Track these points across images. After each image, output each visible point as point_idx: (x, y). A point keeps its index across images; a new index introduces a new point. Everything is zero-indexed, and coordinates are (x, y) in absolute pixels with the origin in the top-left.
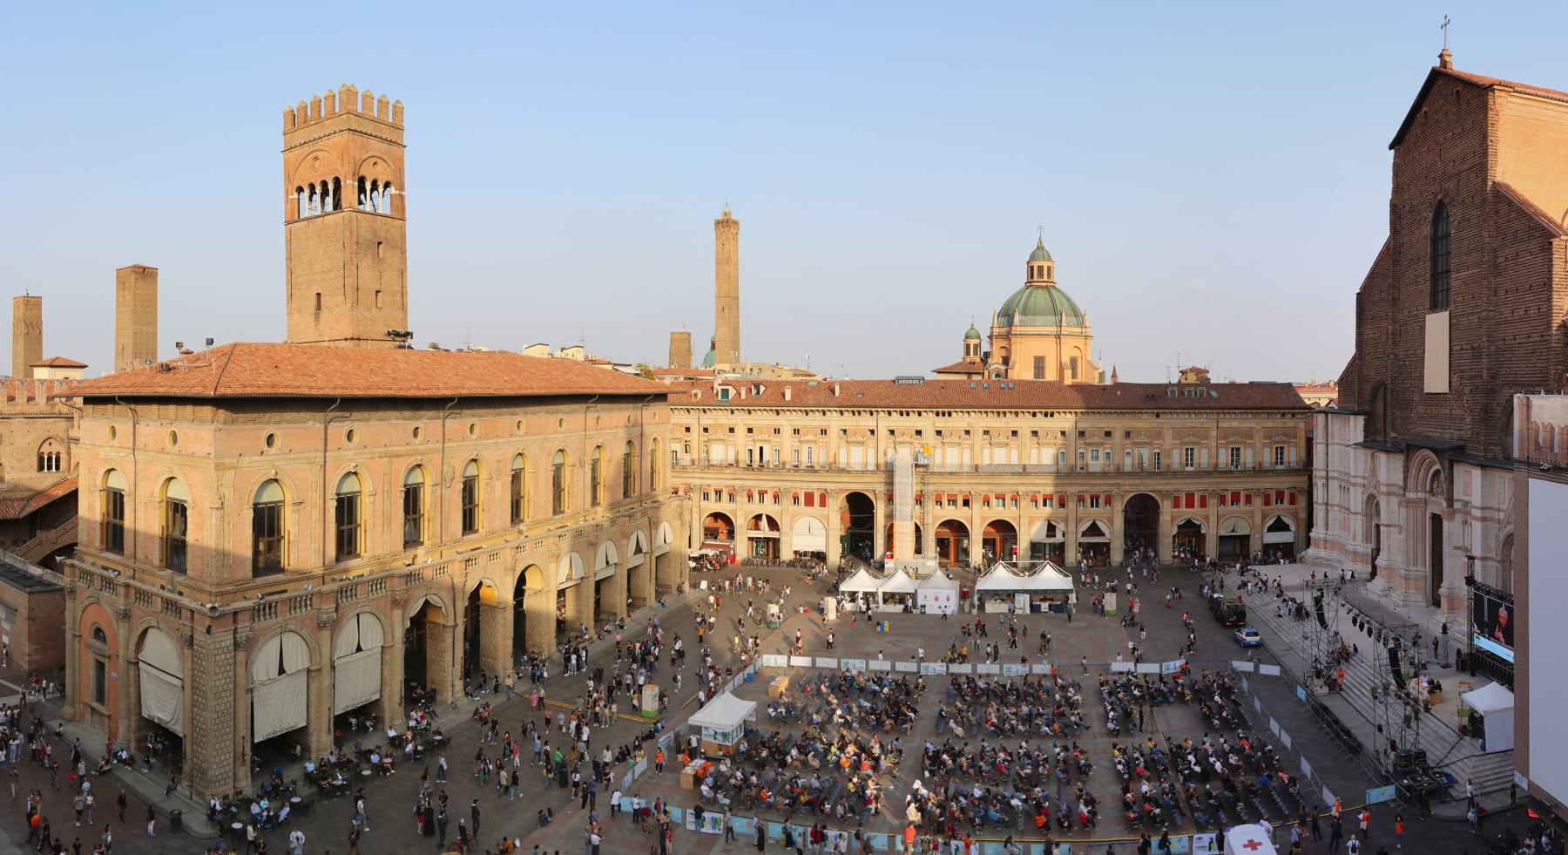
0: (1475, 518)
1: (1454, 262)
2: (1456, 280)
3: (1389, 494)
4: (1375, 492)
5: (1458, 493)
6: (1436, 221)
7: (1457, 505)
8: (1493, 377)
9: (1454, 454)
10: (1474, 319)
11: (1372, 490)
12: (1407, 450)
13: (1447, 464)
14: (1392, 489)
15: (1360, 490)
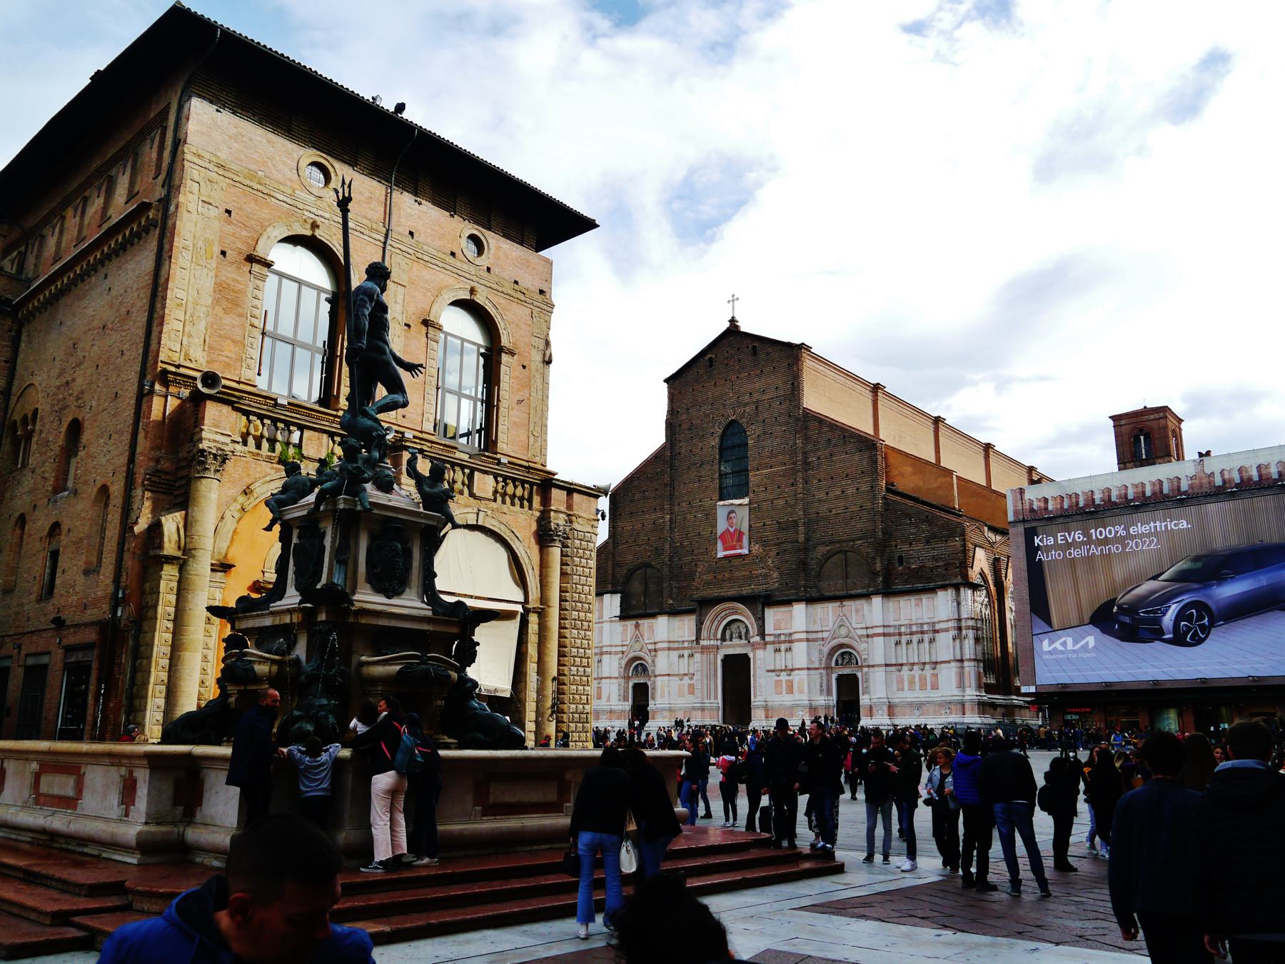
0: (800, 640)
1: (752, 464)
2: (754, 478)
3: (669, 649)
4: (641, 654)
5: (769, 629)
6: (723, 437)
7: (767, 638)
8: (807, 540)
9: (760, 602)
10: (782, 502)
11: (631, 655)
12: (700, 607)
13: (760, 607)
14: (672, 645)
15: (615, 658)
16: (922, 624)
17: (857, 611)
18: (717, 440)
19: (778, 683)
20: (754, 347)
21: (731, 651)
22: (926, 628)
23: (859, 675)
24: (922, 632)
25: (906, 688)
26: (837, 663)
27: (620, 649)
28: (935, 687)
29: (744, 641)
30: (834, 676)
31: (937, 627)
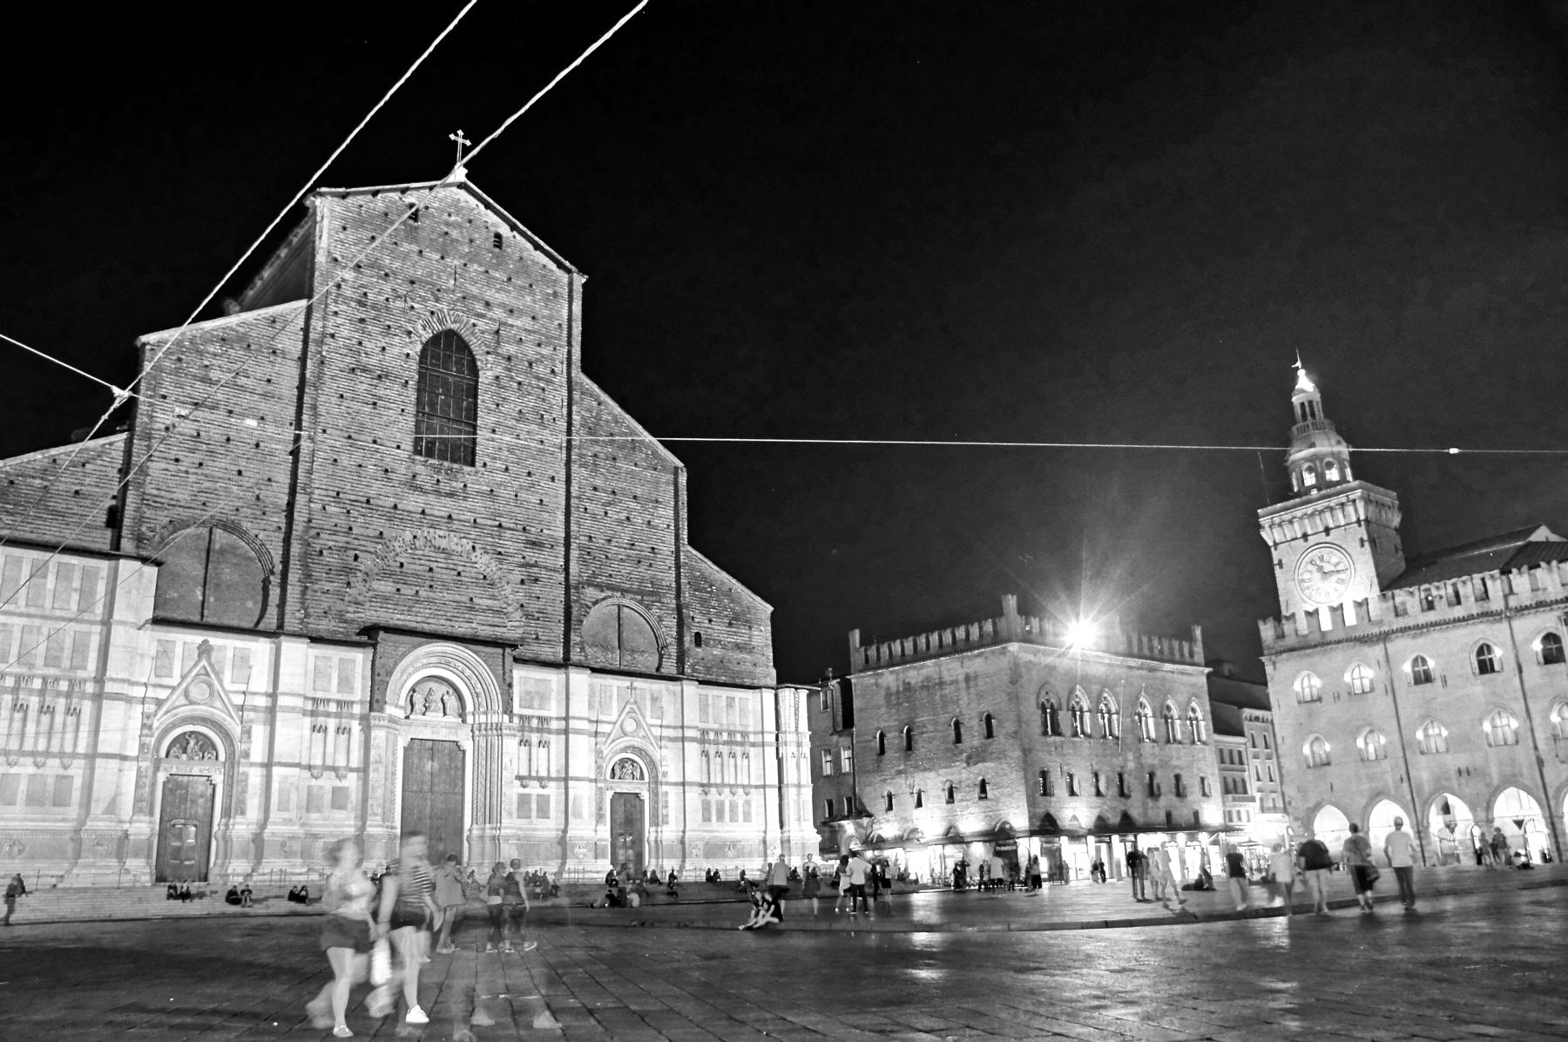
10: (534, 499)
16: (735, 732)
17: (654, 699)
18: (419, 347)
19: (524, 801)
20: (498, 236)
21: (427, 734)
22: (738, 738)
23: (645, 795)
24: (736, 743)
25: (714, 817)
26: (613, 775)
27: (151, 693)
28: (747, 817)
29: (453, 719)
30: (609, 794)
31: (752, 738)
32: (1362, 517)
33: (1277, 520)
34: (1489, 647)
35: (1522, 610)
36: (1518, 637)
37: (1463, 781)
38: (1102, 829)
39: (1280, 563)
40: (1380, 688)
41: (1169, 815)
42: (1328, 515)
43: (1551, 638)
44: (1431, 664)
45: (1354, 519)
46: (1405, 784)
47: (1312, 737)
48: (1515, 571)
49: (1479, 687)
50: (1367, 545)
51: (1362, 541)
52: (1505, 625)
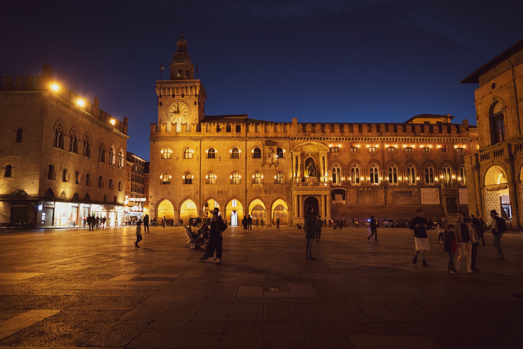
32: (198, 94)
33: (163, 86)
34: (237, 149)
35: (251, 138)
36: (248, 147)
37: (219, 195)
38: (76, 199)
39: (161, 103)
40: (195, 157)
41: (105, 197)
42: (185, 89)
43: (257, 150)
44: (216, 151)
45: (194, 94)
46: (198, 194)
47: (165, 172)
48: (251, 124)
49: (230, 163)
50: (197, 104)
51: (195, 102)
52: (244, 143)
